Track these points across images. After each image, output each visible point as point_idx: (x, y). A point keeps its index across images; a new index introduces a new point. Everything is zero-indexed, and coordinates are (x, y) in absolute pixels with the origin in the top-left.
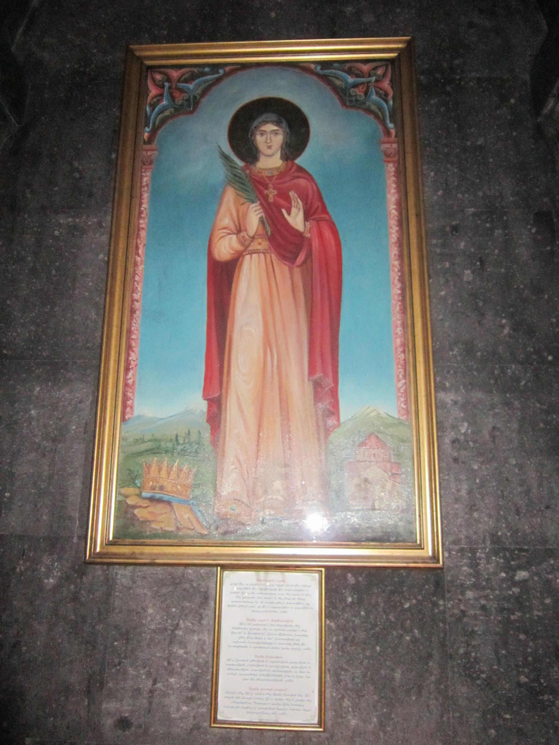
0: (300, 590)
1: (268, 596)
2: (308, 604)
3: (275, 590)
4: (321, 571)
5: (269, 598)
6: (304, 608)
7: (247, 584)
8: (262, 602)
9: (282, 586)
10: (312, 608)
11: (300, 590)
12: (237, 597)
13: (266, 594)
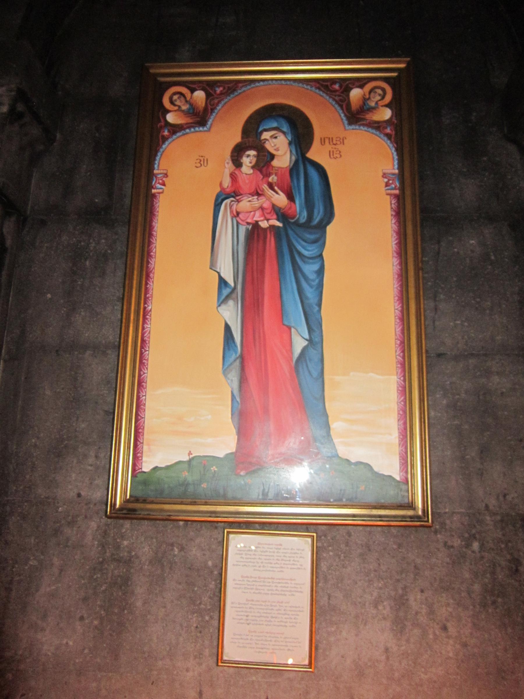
1: (268, 557)
2: (301, 565)
3: (274, 552)
4: (313, 536)
6: (299, 569)
8: (262, 563)
9: (280, 549)
12: (242, 558)
13: (266, 556)
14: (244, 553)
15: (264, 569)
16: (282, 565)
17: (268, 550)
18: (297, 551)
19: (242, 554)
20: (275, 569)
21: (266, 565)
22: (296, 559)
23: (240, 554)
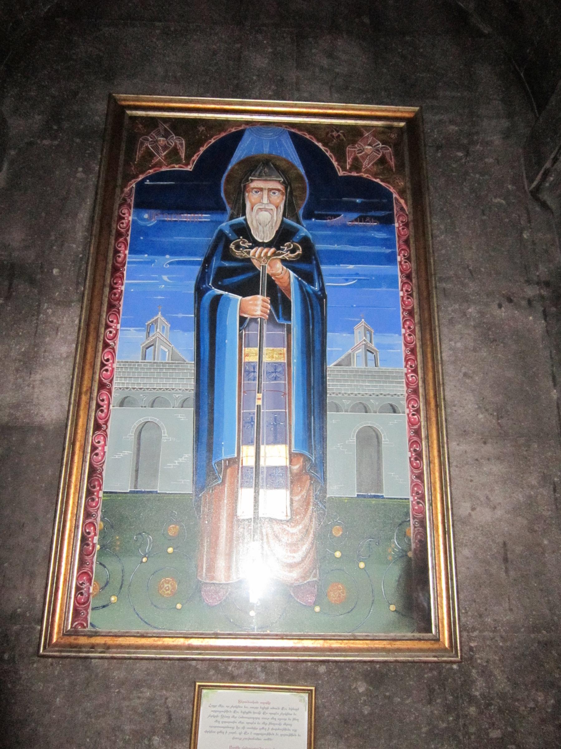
0: (286, 714)
2: (296, 731)
3: (259, 713)
5: (252, 723)
6: (291, 735)
7: (228, 707)
8: (244, 728)
10: (299, 735)
11: (286, 714)
12: (216, 721)
13: (249, 718)
14: (220, 715)
15: (247, 736)
16: (270, 731)
17: (252, 710)
18: (290, 712)
19: (217, 716)
20: (259, 737)
21: (249, 731)
22: (287, 722)
23: (214, 717)
